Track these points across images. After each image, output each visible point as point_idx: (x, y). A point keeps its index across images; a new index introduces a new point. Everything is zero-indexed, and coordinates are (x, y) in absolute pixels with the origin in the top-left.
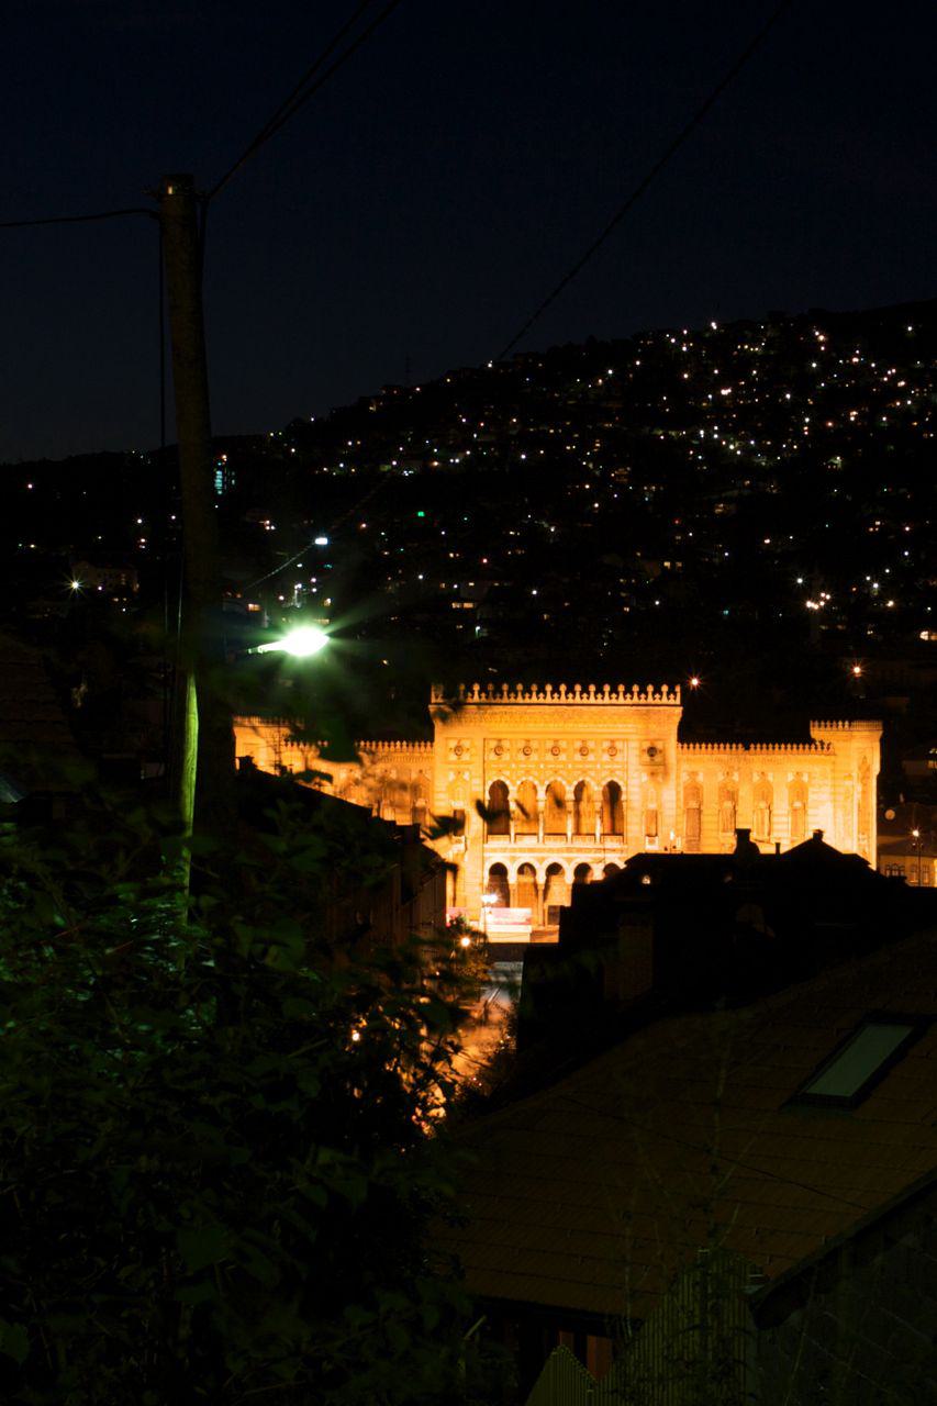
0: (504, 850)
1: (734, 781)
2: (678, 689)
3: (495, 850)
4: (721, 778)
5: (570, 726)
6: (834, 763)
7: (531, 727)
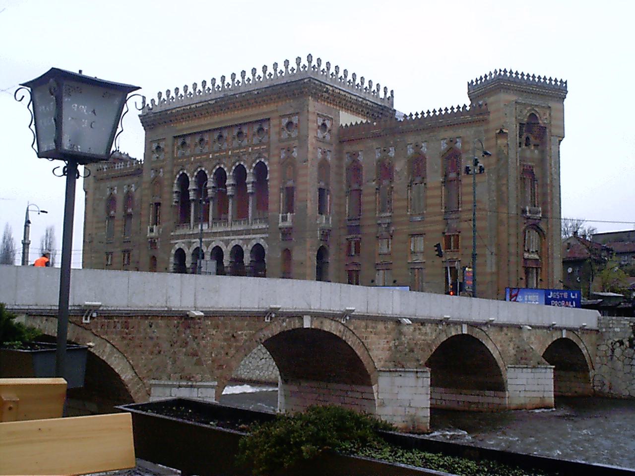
3: (178, 237)
4: (378, 155)
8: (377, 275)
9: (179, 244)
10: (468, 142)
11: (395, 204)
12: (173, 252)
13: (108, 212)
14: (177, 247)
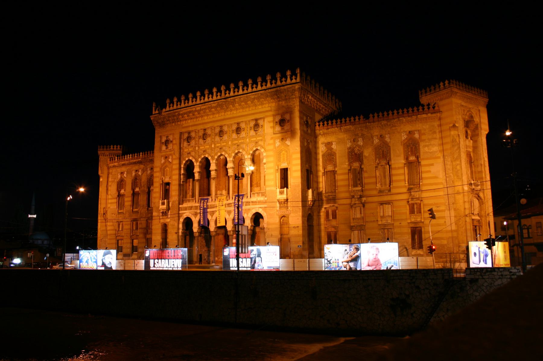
1: (359, 146)
2: (298, 71)
3: (186, 209)
4: (349, 145)
5: (228, 114)
6: (440, 119)
7: (206, 119)
8: (352, 234)
9: (186, 214)
10: (424, 134)
11: (365, 181)
12: (182, 220)
13: (119, 191)
14: (185, 216)
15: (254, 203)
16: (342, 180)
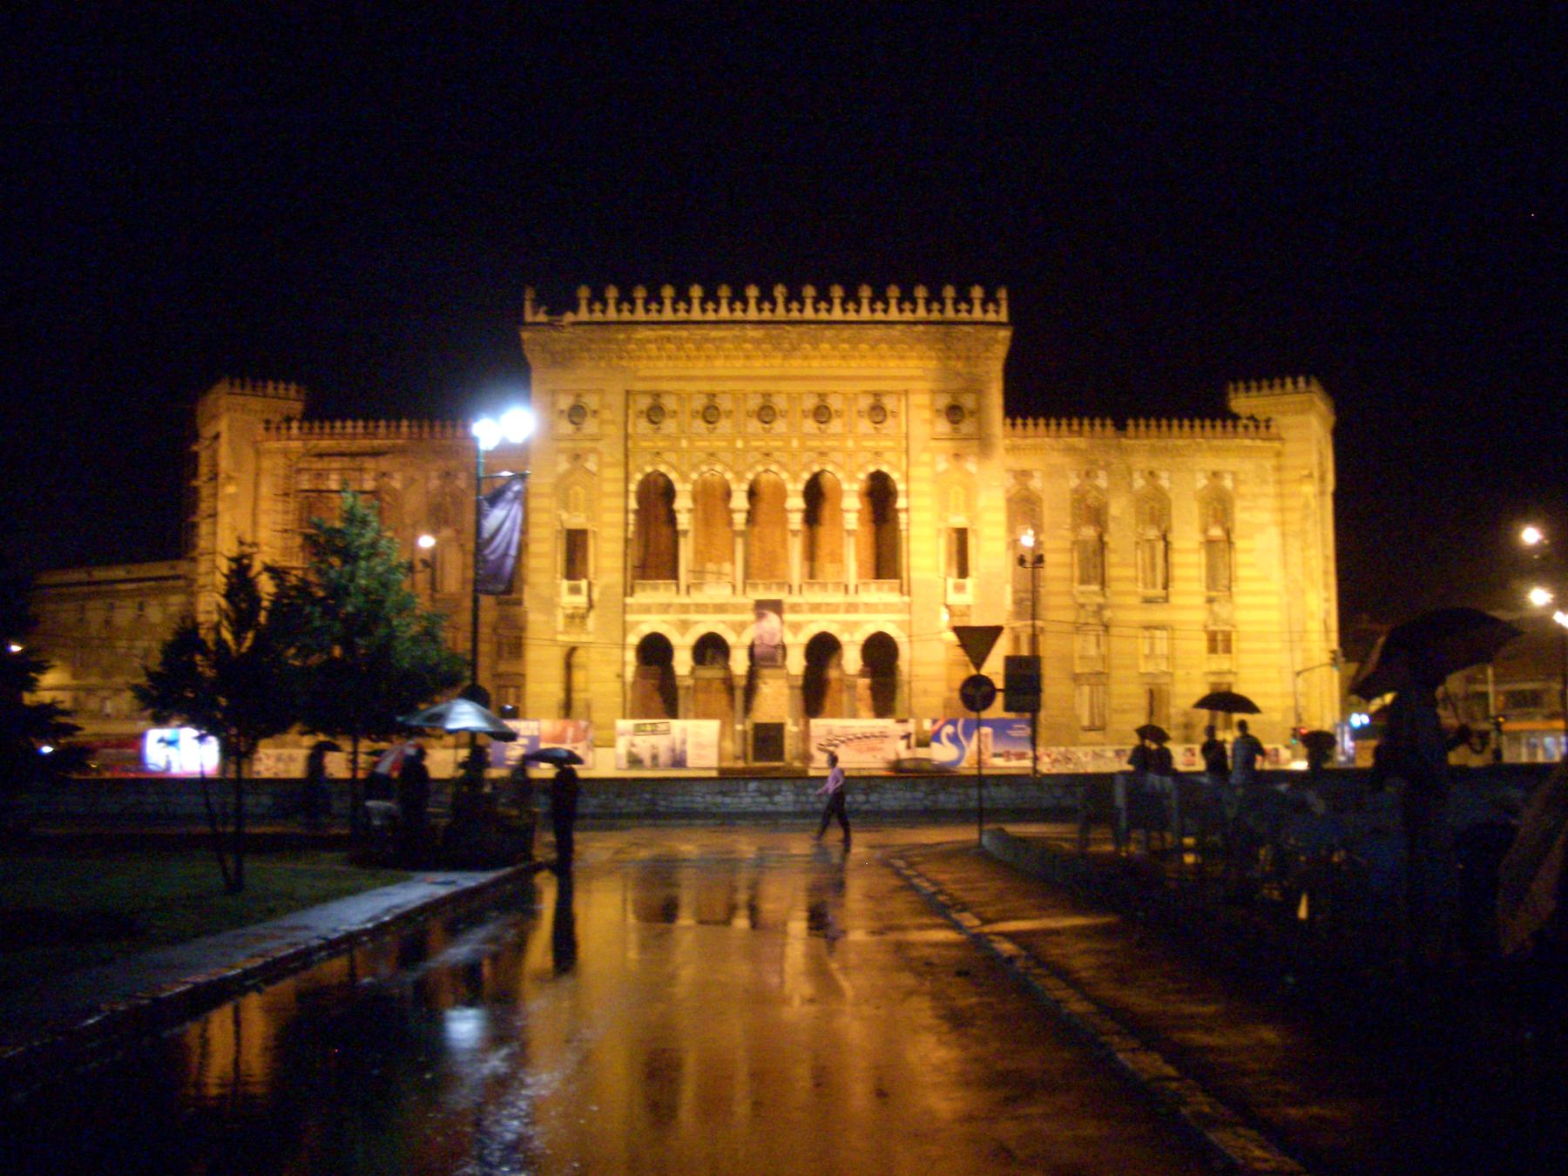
0: (666, 608)
1: (1097, 488)
2: (1002, 294)
3: (647, 609)
4: (1074, 482)
5: (795, 366)
6: (1279, 454)
7: (720, 367)
9: (650, 624)
10: (1244, 482)
11: (1112, 572)
14: (646, 629)
15: (870, 608)
16: (1188, 579)
